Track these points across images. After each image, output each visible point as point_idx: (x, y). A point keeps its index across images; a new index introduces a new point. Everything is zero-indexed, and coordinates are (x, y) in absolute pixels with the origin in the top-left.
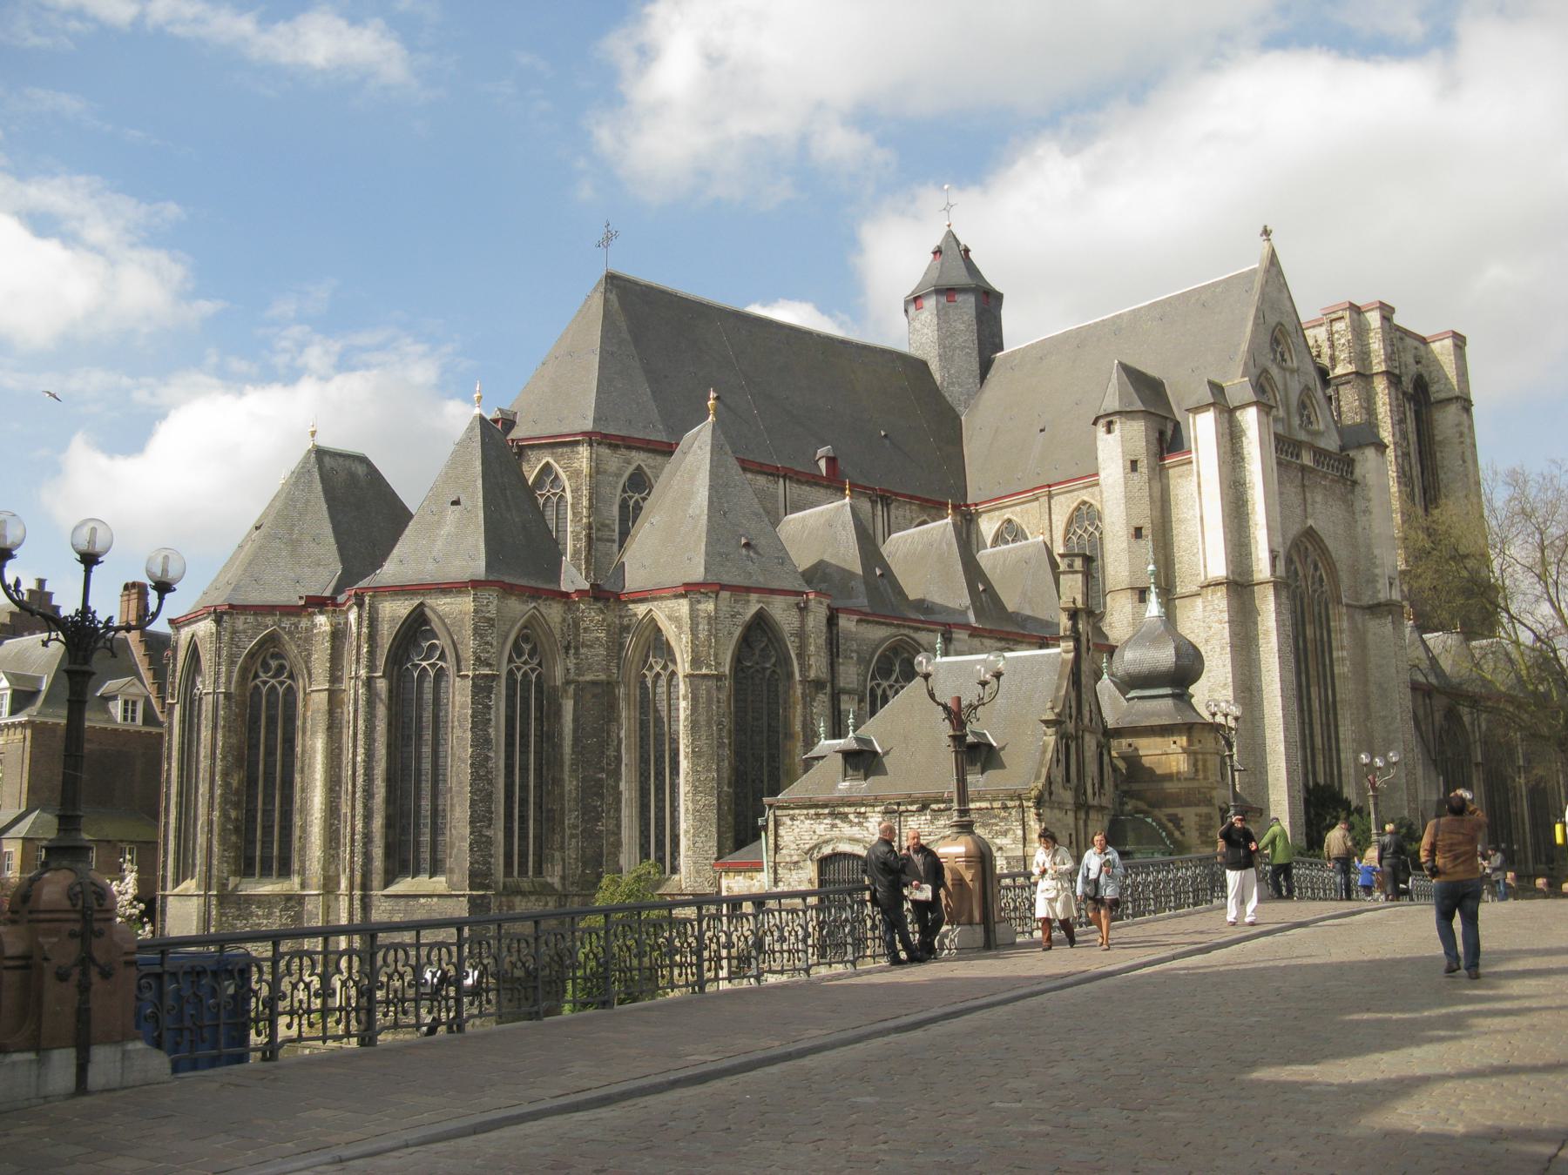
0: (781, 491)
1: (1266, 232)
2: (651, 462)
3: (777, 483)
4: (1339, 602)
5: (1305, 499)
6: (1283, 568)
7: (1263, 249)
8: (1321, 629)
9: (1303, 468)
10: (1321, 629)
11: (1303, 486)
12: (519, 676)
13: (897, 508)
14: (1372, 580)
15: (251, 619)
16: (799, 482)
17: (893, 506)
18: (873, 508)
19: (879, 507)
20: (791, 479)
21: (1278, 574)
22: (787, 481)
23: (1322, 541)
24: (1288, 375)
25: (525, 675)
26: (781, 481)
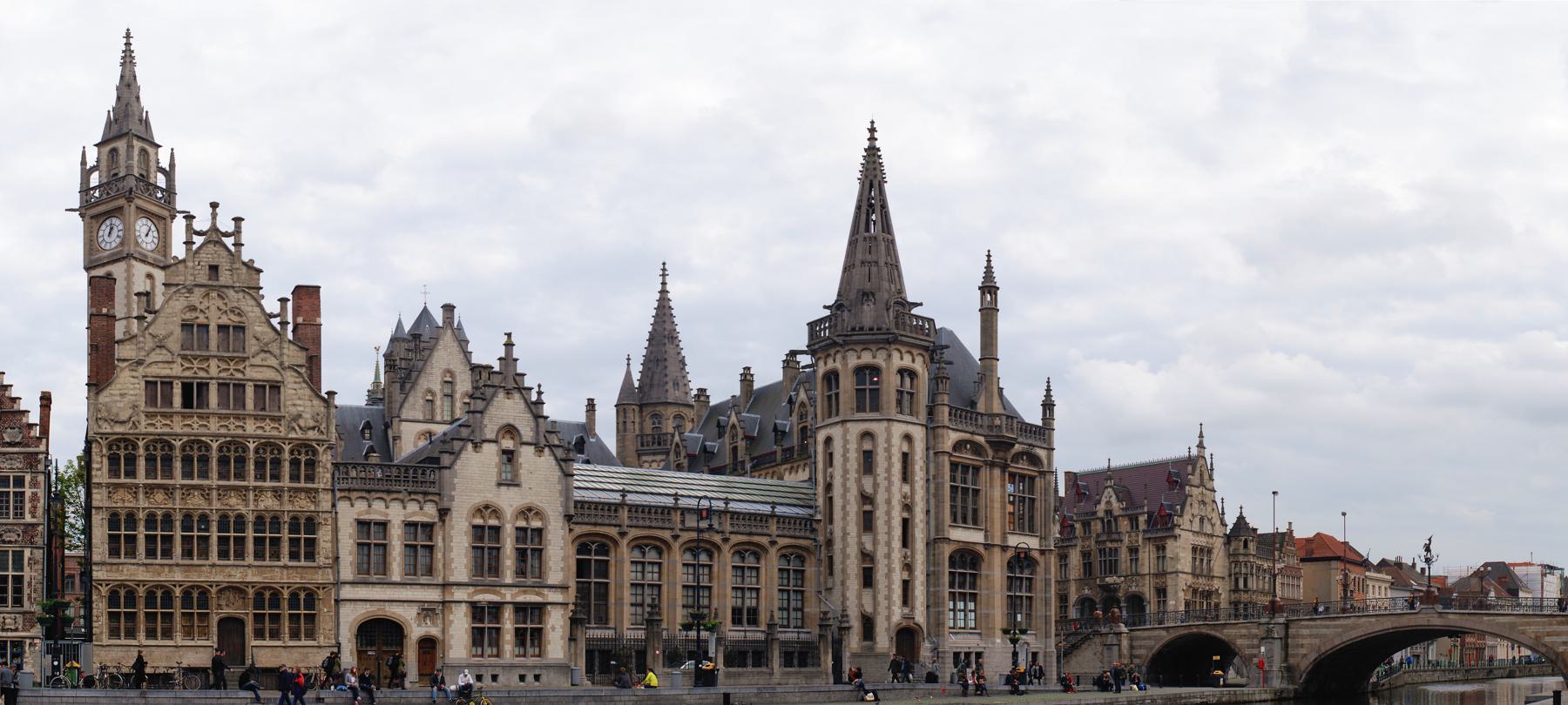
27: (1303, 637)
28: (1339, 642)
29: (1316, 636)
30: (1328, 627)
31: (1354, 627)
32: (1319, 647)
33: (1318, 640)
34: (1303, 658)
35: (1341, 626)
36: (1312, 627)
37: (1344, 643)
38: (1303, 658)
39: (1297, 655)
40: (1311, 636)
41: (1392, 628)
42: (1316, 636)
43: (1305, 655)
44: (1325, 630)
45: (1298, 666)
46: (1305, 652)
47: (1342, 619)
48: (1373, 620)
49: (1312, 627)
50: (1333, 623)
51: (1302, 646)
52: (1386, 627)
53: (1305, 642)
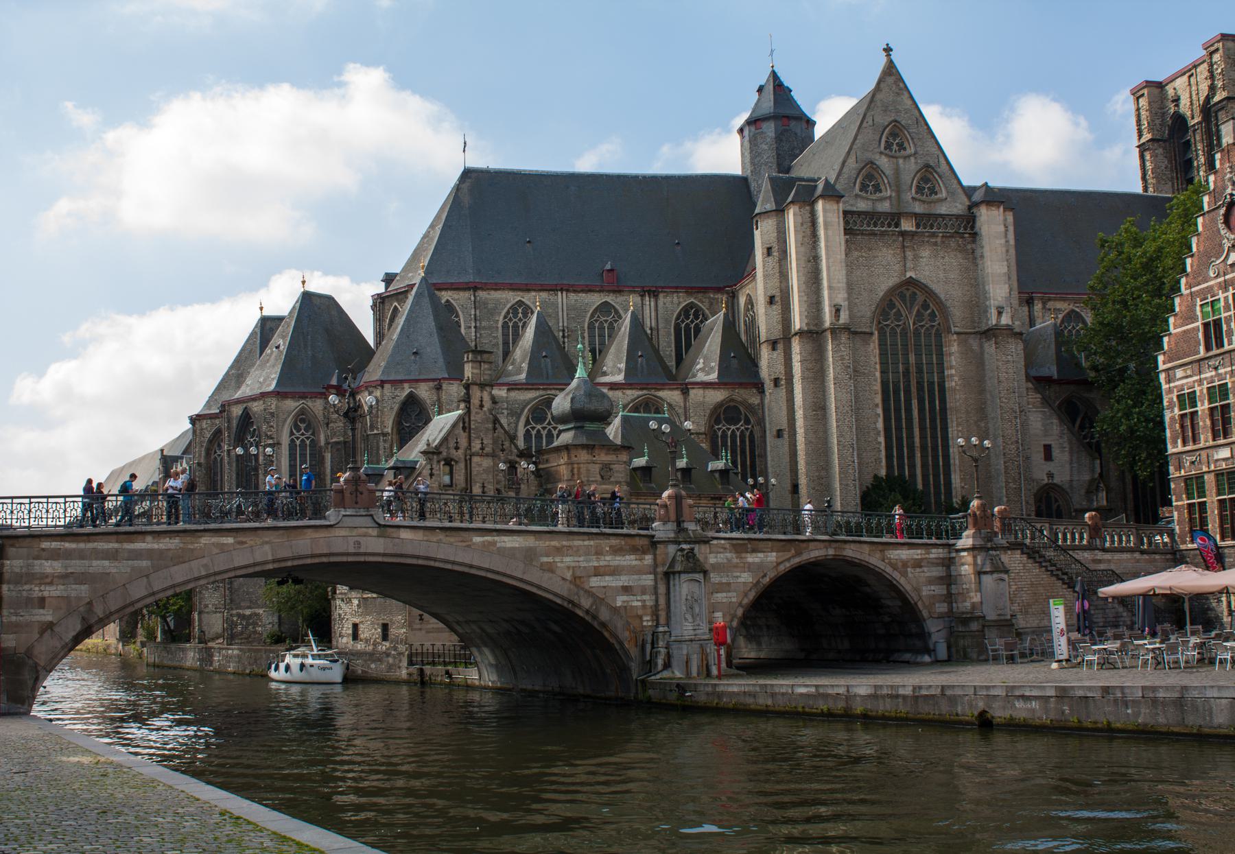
0: (560, 300)
1: (888, 50)
2: (456, 296)
3: (557, 295)
4: (949, 331)
5: (905, 258)
6: (847, 317)
7: (882, 61)
8: (929, 354)
9: (903, 234)
10: (929, 354)
11: (903, 247)
12: (298, 442)
13: (665, 297)
14: (986, 311)
15: (209, 422)
16: (575, 291)
17: (661, 295)
18: (642, 300)
19: (647, 298)
20: (567, 291)
21: (842, 321)
22: (564, 293)
23: (926, 287)
24: (901, 161)
25: (303, 441)
26: (559, 293)
27: (45, 579)
28: (144, 593)
29: (81, 578)
30: (113, 556)
31: (179, 558)
32: (90, 603)
33: (84, 588)
34: (42, 633)
35: (150, 554)
36: (68, 555)
37: (153, 594)
38: (42, 633)
39: (29, 625)
40: (65, 577)
41: (274, 561)
42: (81, 578)
43: (50, 626)
44: (106, 563)
45: (29, 653)
46: (49, 618)
47: (149, 538)
48: (230, 540)
49: (68, 555)
50: (90, 545)
51: (42, 602)
52: (259, 559)
53: (51, 591)
